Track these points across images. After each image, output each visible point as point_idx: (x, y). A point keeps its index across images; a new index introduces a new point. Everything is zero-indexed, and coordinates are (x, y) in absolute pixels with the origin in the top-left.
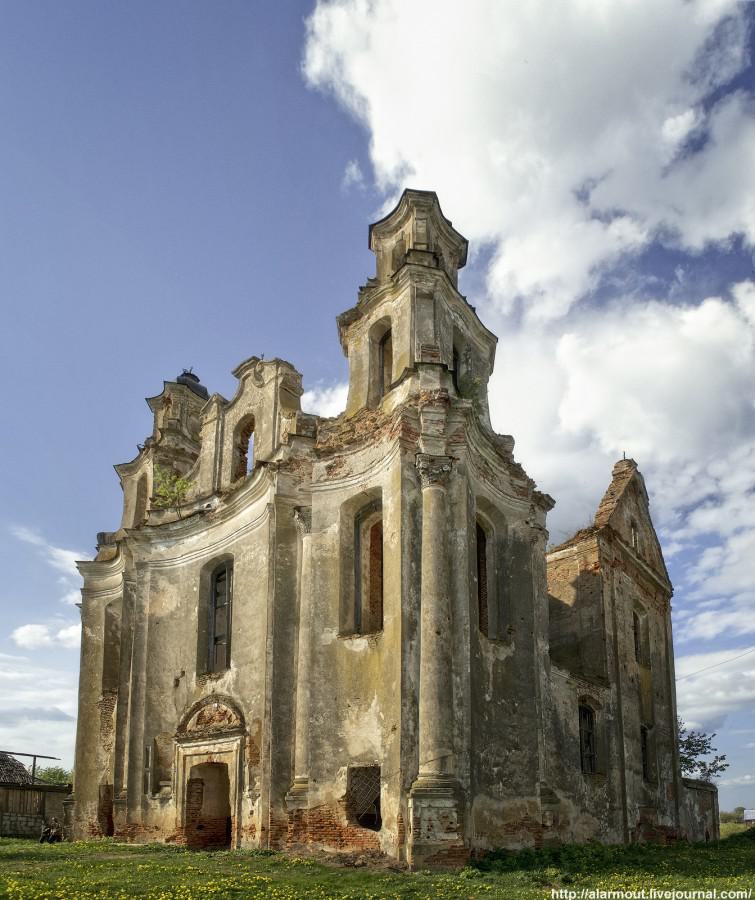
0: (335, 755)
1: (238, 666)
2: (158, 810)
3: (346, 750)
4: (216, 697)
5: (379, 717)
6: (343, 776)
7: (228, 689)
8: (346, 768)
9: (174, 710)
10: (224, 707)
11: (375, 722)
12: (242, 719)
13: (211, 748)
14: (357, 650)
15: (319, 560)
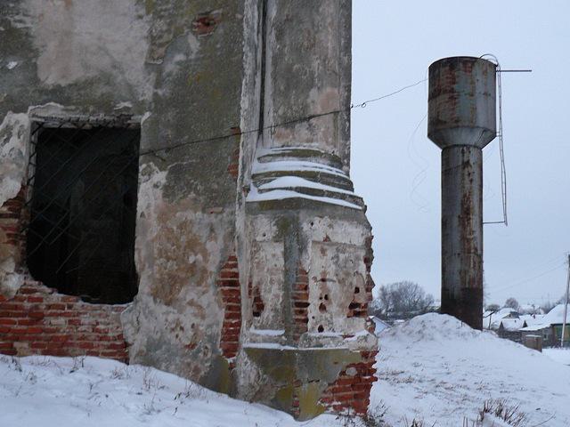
3: (31, 67)
6: (15, 142)
8: (24, 119)
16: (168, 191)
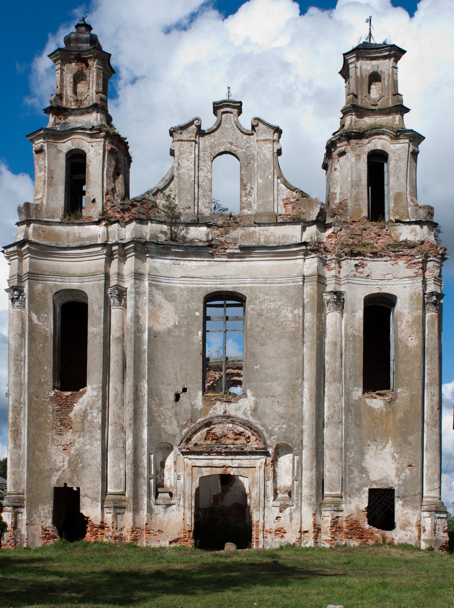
0: (360, 479)
1: (256, 395)
2: (161, 516)
3: (368, 476)
4: (227, 417)
5: (394, 457)
7: (245, 414)
8: (367, 489)
9: (175, 423)
10: (241, 429)
11: (389, 458)
12: (265, 443)
13: (228, 463)
14: (376, 407)
15: (351, 336)
16: (403, 506)
